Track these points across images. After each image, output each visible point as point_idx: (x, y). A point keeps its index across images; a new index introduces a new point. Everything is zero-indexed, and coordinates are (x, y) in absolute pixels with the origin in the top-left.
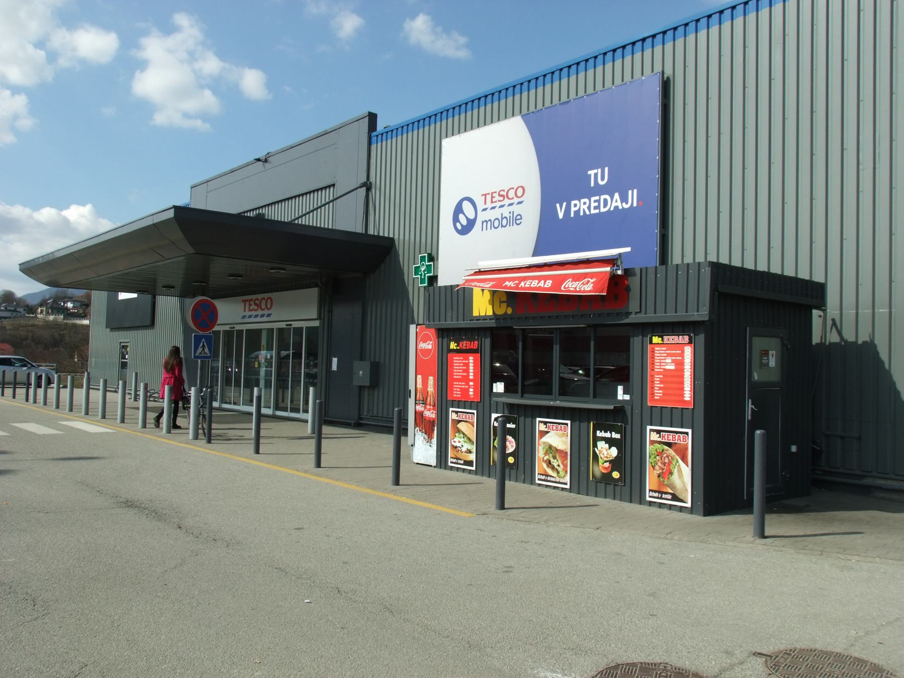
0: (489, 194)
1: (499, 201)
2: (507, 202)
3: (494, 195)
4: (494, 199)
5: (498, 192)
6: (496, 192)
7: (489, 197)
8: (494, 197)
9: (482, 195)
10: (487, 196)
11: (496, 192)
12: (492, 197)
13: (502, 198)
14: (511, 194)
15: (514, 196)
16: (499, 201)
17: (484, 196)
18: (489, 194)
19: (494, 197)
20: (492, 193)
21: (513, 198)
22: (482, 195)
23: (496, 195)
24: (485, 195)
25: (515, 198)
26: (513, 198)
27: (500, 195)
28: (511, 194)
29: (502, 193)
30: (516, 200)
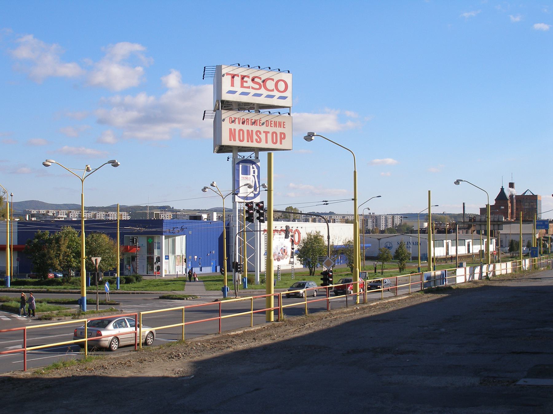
1: (253, 88)
2: (263, 91)
3: (245, 79)
8: (246, 82)
11: (248, 77)
13: (257, 86)
14: (270, 85)
15: (273, 87)
16: (253, 88)
18: (238, 76)
19: (246, 82)
20: (243, 78)
21: (273, 90)
23: (249, 80)
25: (275, 90)
26: (273, 90)
29: (256, 80)
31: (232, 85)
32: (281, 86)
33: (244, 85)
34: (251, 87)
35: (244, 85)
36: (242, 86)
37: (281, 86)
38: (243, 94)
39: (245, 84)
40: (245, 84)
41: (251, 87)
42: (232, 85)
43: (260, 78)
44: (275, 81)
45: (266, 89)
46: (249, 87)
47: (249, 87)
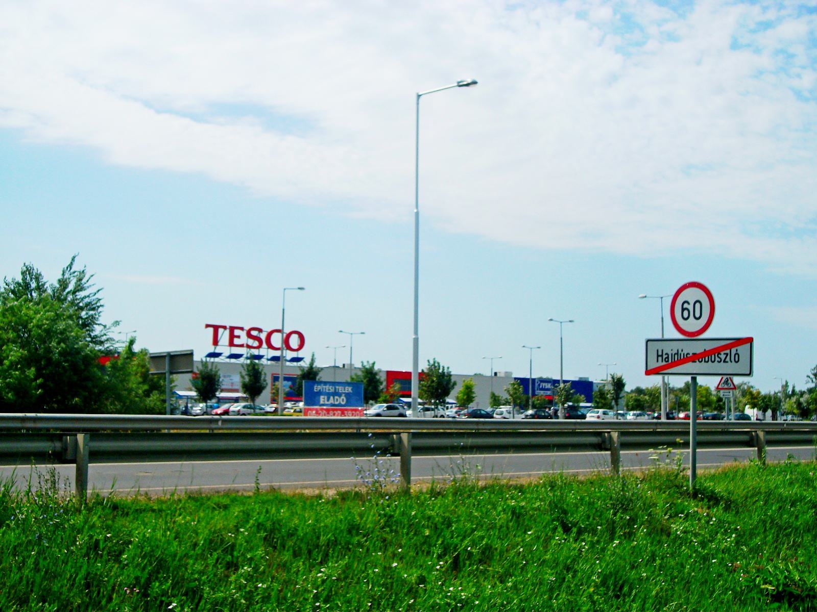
0: (225, 328)
3: (237, 332)
6: (242, 329)
7: (224, 336)
8: (239, 337)
9: (208, 326)
10: (221, 331)
11: (242, 329)
12: (232, 336)
13: (256, 344)
14: (277, 340)
16: (249, 347)
17: (211, 330)
19: (239, 337)
20: (232, 329)
22: (208, 326)
23: (243, 334)
24: (216, 328)
27: (249, 335)
28: (277, 340)
29: (254, 333)
31: (216, 342)
32: (294, 341)
34: (245, 345)
36: (231, 344)
40: (236, 341)
42: (216, 342)
43: (260, 330)
45: (270, 346)
46: (242, 346)
47: (242, 346)
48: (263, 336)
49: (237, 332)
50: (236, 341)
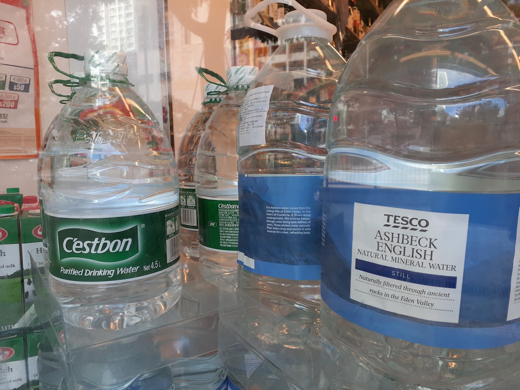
0: (392, 216)
1: (402, 223)
2: (409, 225)
3: (397, 218)
4: (396, 221)
5: (401, 217)
6: (399, 217)
7: (392, 219)
8: (398, 220)
9: (385, 215)
10: (390, 217)
11: (399, 217)
12: (395, 219)
13: (405, 223)
14: (415, 222)
16: (402, 223)
18: (392, 216)
19: (398, 220)
20: (395, 217)
21: (416, 226)
22: (385, 215)
23: (400, 219)
24: (389, 216)
25: (418, 225)
26: (416, 226)
27: (402, 219)
30: (418, 227)
31: (388, 221)
32: (423, 223)
33: (396, 222)
35: (396, 222)
36: (395, 222)
37: (423, 223)
38: (394, 227)
39: (397, 221)
41: (400, 223)
42: (388, 221)
43: (408, 218)
44: (419, 220)
46: (399, 223)
47: (399, 223)
48: (409, 220)
49: (397, 218)
50: (397, 221)
